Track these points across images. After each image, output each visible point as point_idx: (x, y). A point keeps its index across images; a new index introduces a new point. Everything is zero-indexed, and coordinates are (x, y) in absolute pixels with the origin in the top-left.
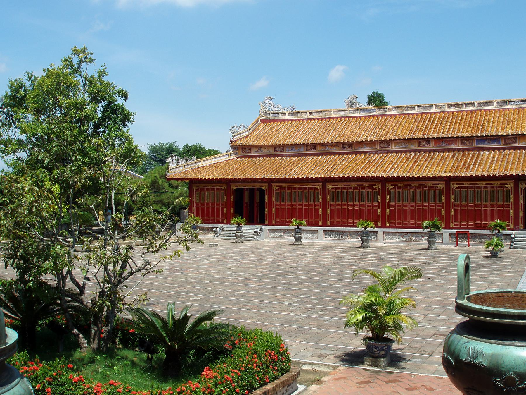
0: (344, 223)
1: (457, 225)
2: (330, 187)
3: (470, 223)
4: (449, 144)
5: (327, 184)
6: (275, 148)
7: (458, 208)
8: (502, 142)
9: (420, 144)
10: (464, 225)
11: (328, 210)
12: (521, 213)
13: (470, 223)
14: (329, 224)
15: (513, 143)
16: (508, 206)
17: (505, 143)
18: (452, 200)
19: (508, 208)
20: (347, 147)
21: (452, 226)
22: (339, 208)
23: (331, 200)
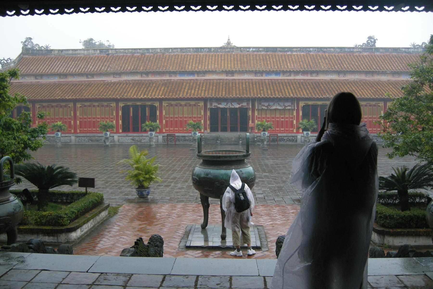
0: (90, 131)
1: (167, 130)
2: (78, 105)
3: (176, 129)
4: (161, 76)
5: (77, 104)
6: (36, 77)
7: (168, 119)
8: (196, 76)
9: (141, 76)
10: (172, 130)
11: (78, 122)
12: (208, 122)
13: (176, 129)
14: (78, 132)
15: (203, 76)
16: (200, 118)
17: (198, 76)
18: (164, 113)
19: (200, 119)
20: (90, 76)
21: (164, 131)
22: (86, 120)
23: (80, 115)
